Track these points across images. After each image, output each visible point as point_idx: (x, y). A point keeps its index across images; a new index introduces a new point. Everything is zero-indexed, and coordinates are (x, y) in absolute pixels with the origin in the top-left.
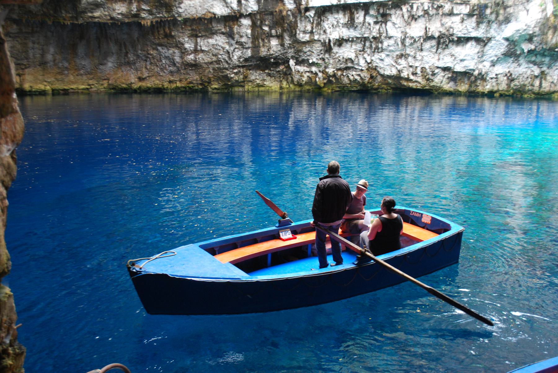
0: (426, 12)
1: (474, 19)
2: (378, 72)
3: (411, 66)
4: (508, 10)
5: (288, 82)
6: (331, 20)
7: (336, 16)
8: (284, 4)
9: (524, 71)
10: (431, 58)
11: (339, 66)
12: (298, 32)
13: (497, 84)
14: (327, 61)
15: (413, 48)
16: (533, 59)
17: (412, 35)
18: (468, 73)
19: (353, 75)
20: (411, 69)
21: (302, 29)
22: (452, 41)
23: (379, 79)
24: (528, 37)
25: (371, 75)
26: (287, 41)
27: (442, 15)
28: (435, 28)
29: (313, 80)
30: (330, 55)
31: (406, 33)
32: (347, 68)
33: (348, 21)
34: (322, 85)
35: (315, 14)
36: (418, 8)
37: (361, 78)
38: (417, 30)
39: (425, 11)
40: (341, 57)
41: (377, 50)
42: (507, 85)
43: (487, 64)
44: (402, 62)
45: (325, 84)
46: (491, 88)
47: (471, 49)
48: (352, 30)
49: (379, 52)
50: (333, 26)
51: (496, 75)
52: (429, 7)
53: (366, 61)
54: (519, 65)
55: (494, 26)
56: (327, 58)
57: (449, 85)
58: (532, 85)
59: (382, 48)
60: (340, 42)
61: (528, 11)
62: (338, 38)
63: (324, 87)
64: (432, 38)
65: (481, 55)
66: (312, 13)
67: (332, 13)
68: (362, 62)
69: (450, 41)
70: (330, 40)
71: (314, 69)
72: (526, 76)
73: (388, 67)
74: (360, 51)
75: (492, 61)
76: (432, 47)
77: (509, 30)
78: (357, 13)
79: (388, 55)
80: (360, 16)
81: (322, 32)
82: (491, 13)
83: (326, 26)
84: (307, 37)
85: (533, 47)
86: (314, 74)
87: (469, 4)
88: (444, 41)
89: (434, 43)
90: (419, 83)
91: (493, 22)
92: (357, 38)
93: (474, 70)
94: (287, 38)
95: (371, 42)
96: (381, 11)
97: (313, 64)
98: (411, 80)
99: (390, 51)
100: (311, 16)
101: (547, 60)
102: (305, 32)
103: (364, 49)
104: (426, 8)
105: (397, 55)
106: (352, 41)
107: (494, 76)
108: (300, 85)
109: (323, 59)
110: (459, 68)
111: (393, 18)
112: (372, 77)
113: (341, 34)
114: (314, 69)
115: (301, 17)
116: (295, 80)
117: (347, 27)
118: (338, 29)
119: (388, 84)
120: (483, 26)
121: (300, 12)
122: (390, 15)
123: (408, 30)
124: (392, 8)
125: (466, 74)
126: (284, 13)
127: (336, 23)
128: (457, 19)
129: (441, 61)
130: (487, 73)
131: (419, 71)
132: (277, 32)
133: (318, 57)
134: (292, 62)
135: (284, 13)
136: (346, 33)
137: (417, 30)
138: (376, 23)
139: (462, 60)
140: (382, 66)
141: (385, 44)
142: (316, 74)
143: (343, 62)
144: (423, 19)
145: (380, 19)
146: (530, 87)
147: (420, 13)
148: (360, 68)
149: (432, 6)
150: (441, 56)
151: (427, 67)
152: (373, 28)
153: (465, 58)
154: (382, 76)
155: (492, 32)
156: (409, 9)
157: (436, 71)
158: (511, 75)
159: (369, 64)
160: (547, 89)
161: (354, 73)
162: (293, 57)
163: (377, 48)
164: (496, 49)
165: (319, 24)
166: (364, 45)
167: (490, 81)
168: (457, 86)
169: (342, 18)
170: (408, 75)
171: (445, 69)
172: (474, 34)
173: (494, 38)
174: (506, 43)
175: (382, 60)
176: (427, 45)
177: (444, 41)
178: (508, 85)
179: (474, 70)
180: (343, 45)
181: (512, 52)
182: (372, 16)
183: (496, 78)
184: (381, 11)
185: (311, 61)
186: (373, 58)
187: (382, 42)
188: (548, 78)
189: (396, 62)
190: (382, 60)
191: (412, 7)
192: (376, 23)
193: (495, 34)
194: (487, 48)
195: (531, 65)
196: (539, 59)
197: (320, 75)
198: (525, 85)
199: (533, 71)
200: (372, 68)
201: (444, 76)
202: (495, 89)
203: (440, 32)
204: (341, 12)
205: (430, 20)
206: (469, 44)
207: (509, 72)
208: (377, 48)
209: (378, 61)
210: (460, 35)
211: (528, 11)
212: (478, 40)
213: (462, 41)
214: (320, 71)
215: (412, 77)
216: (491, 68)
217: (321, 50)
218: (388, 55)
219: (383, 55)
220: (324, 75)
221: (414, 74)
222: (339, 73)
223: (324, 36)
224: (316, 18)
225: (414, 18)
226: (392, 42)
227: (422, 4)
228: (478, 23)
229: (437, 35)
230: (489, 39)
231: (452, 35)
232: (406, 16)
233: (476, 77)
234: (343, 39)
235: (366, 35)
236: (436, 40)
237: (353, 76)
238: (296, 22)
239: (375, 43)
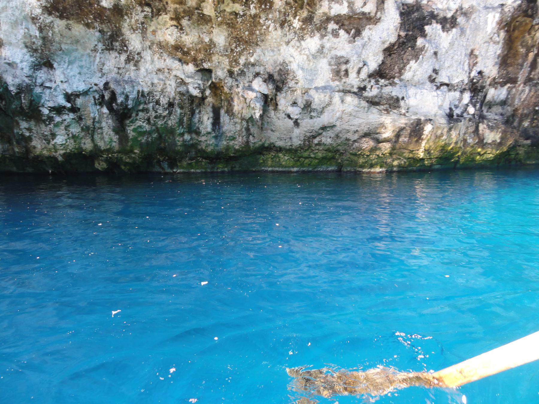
46: (71, 145)
51: (68, 97)
58: (193, 130)
72: (164, 101)
107: (62, 101)
146: (187, 137)
160: (238, 144)
167: (58, 119)
178: (120, 129)
183: (74, 110)
198: (171, 131)
199: (183, 83)
202: (87, 145)
207: (106, 84)
216: (42, 75)
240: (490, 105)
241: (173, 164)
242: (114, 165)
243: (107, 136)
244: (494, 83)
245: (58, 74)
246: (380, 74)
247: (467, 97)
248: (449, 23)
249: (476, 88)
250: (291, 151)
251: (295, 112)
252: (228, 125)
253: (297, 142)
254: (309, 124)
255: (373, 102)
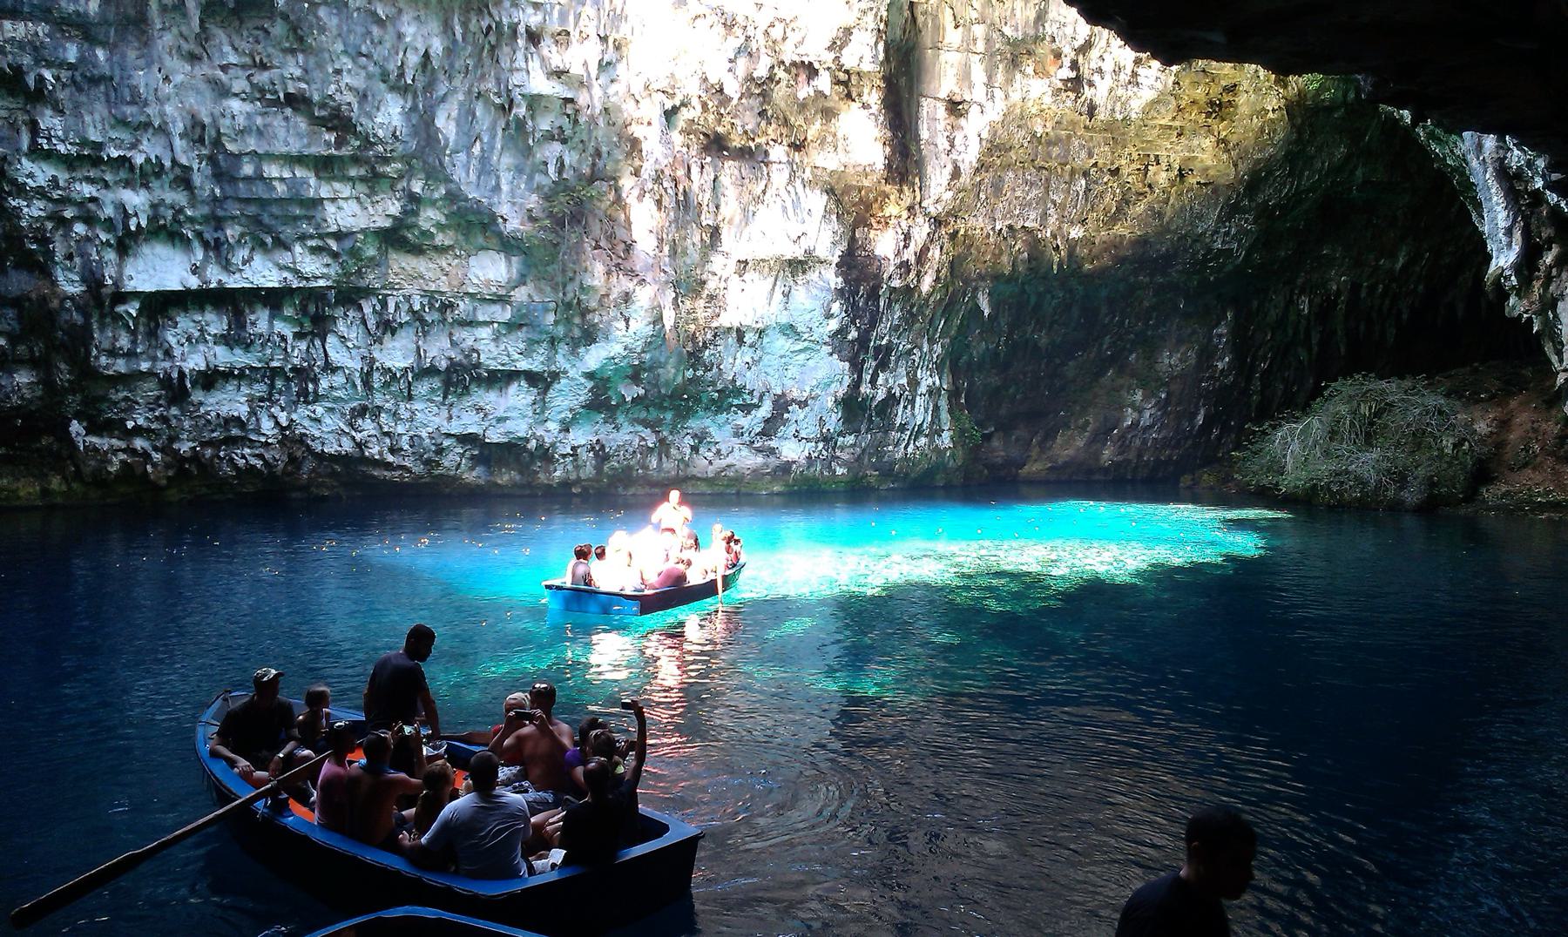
0: (417, 316)
1: (521, 334)
2: (308, 447)
3: (387, 434)
4: (589, 317)
5: (64, 478)
6: (186, 322)
7: (198, 318)
8: (54, 283)
9: (625, 436)
10: (430, 418)
11: (207, 435)
12: (95, 352)
13: (577, 468)
14: (174, 423)
15: (390, 393)
16: (643, 415)
17: (388, 364)
18: (516, 445)
19: (245, 456)
20: (388, 441)
21: (106, 345)
22: (479, 380)
23: (309, 465)
24: (630, 371)
25: (290, 455)
26: (64, 373)
27: (451, 324)
28: (438, 350)
29: (139, 471)
30: (182, 409)
31: (373, 360)
32: (231, 441)
33: (230, 328)
34: (164, 482)
35: (140, 311)
36: (397, 307)
37: (266, 463)
38: (396, 354)
39: (414, 313)
40: (213, 414)
41: (306, 397)
42: (595, 468)
43: (553, 426)
44: (368, 425)
45: (169, 478)
47: (518, 397)
48: (238, 351)
49: (307, 403)
50: (189, 339)
51: (573, 448)
52: (423, 306)
53: (277, 423)
54: (617, 428)
55: (563, 349)
56: (175, 417)
57: (474, 474)
58: (645, 468)
59: (315, 392)
60: (210, 379)
61: (627, 320)
62: (203, 367)
63: (167, 487)
64: (432, 371)
65: (541, 406)
66: (133, 308)
67: (186, 310)
68: (267, 425)
69: (472, 379)
70: (182, 374)
71: (139, 443)
73: (330, 437)
74: (262, 400)
75: (562, 422)
76: (433, 390)
77: (594, 357)
78: (253, 313)
79: (331, 410)
80: (260, 321)
81: (160, 354)
82: (556, 323)
83: (173, 341)
84: (121, 366)
85: (642, 392)
86: (140, 455)
87: (510, 303)
88: (461, 378)
89: (437, 383)
90: (408, 470)
91: (561, 340)
92: (252, 368)
93: (527, 440)
94: (63, 366)
95: (288, 379)
96: (312, 309)
97: (138, 431)
98: (390, 464)
99: (337, 400)
100: (130, 314)
101: (669, 416)
102: (113, 353)
103: (271, 394)
104: (417, 307)
105: (353, 410)
106: (241, 376)
108: (100, 480)
109: (164, 419)
110: (495, 436)
111: (341, 327)
112: (292, 459)
113: (211, 359)
114: (139, 443)
115: (102, 316)
116: (87, 470)
117: (227, 344)
118: (202, 347)
119: (333, 474)
120: (542, 349)
121: (99, 303)
122: (334, 319)
123: (376, 355)
124: (337, 303)
125: (512, 451)
126: (55, 303)
127: (197, 334)
128: (485, 333)
129: (454, 423)
130: (553, 445)
131: (404, 443)
132: (31, 350)
133: (150, 415)
134: (76, 427)
135: (55, 303)
136: (223, 357)
137: (396, 354)
138: (299, 336)
139: (500, 420)
140: (317, 434)
141: (324, 384)
142: (146, 455)
143: (219, 425)
144: (412, 331)
145: (308, 326)
147: (405, 318)
148: (263, 439)
149: (431, 306)
150: (455, 411)
151: (424, 435)
152: (293, 348)
153: (508, 414)
154: (321, 457)
155: (561, 362)
156: (378, 308)
157: (446, 443)
158: (603, 447)
159: (283, 429)
161: (247, 451)
162: (79, 416)
163: (303, 393)
164: (567, 397)
165: (153, 334)
166: (272, 386)
168: (491, 474)
169: (216, 323)
170: (381, 453)
171: (466, 439)
172: (523, 365)
173: (565, 372)
174: (590, 385)
175: (318, 421)
176: (422, 388)
177: (461, 378)
178: (599, 468)
179: (527, 440)
180: (218, 385)
181: (600, 402)
182: (286, 319)
184: (312, 309)
185: (130, 424)
186: (294, 416)
187: (316, 381)
188: (673, 451)
189: (351, 425)
190: (318, 421)
191: (384, 304)
192: (299, 336)
193: (568, 366)
194: (551, 393)
195: (640, 428)
196: (654, 414)
197: (157, 456)
198: (630, 468)
200: (291, 439)
201: (462, 455)
202: (573, 477)
203: (450, 359)
204: (209, 308)
205: (425, 334)
206: (513, 388)
208: (303, 393)
209: (306, 423)
210: (493, 365)
211: (627, 320)
212: (532, 378)
213: (500, 379)
214: (156, 449)
215: (390, 458)
217: (159, 398)
218: (331, 410)
219: (320, 410)
220: (168, 459)
221: (392, 451)
222: (209, 452)
223: (167, 365)
224: (142, 320)
225: (388, 327)
226: (339, 379)
227: (408, 298)
228: (532, 343)
229: (444, 364)
230: (555, 376)
231: (478, 365)
232: (371, 323)
233: (531, 453)
234: (216, 371)
235: (275, 364)
236: (443, 377)
237: (243, 457)
238: (87, 328)
239: (302, 382)
240: (842, 448)
241: (625, 488)
242: (585, 489)
243: (588, 471)
244: (841, 434)
245: (571, 435)
246: (762, 433)
247: (821, 445)
248: (803, 404)
249: (826, 439)
250: (709, 481)
251: (710, 455)
252: (666, 465)
253: (711, 475)
254: (720, 463)
255: (759, 450)
